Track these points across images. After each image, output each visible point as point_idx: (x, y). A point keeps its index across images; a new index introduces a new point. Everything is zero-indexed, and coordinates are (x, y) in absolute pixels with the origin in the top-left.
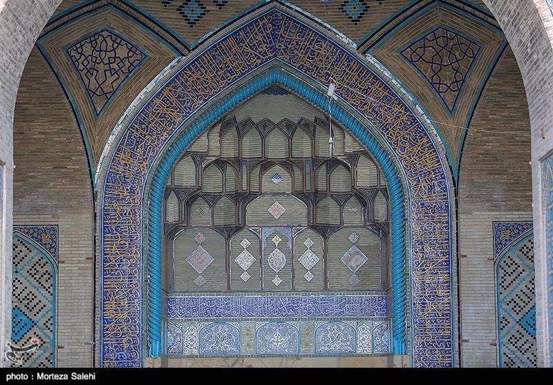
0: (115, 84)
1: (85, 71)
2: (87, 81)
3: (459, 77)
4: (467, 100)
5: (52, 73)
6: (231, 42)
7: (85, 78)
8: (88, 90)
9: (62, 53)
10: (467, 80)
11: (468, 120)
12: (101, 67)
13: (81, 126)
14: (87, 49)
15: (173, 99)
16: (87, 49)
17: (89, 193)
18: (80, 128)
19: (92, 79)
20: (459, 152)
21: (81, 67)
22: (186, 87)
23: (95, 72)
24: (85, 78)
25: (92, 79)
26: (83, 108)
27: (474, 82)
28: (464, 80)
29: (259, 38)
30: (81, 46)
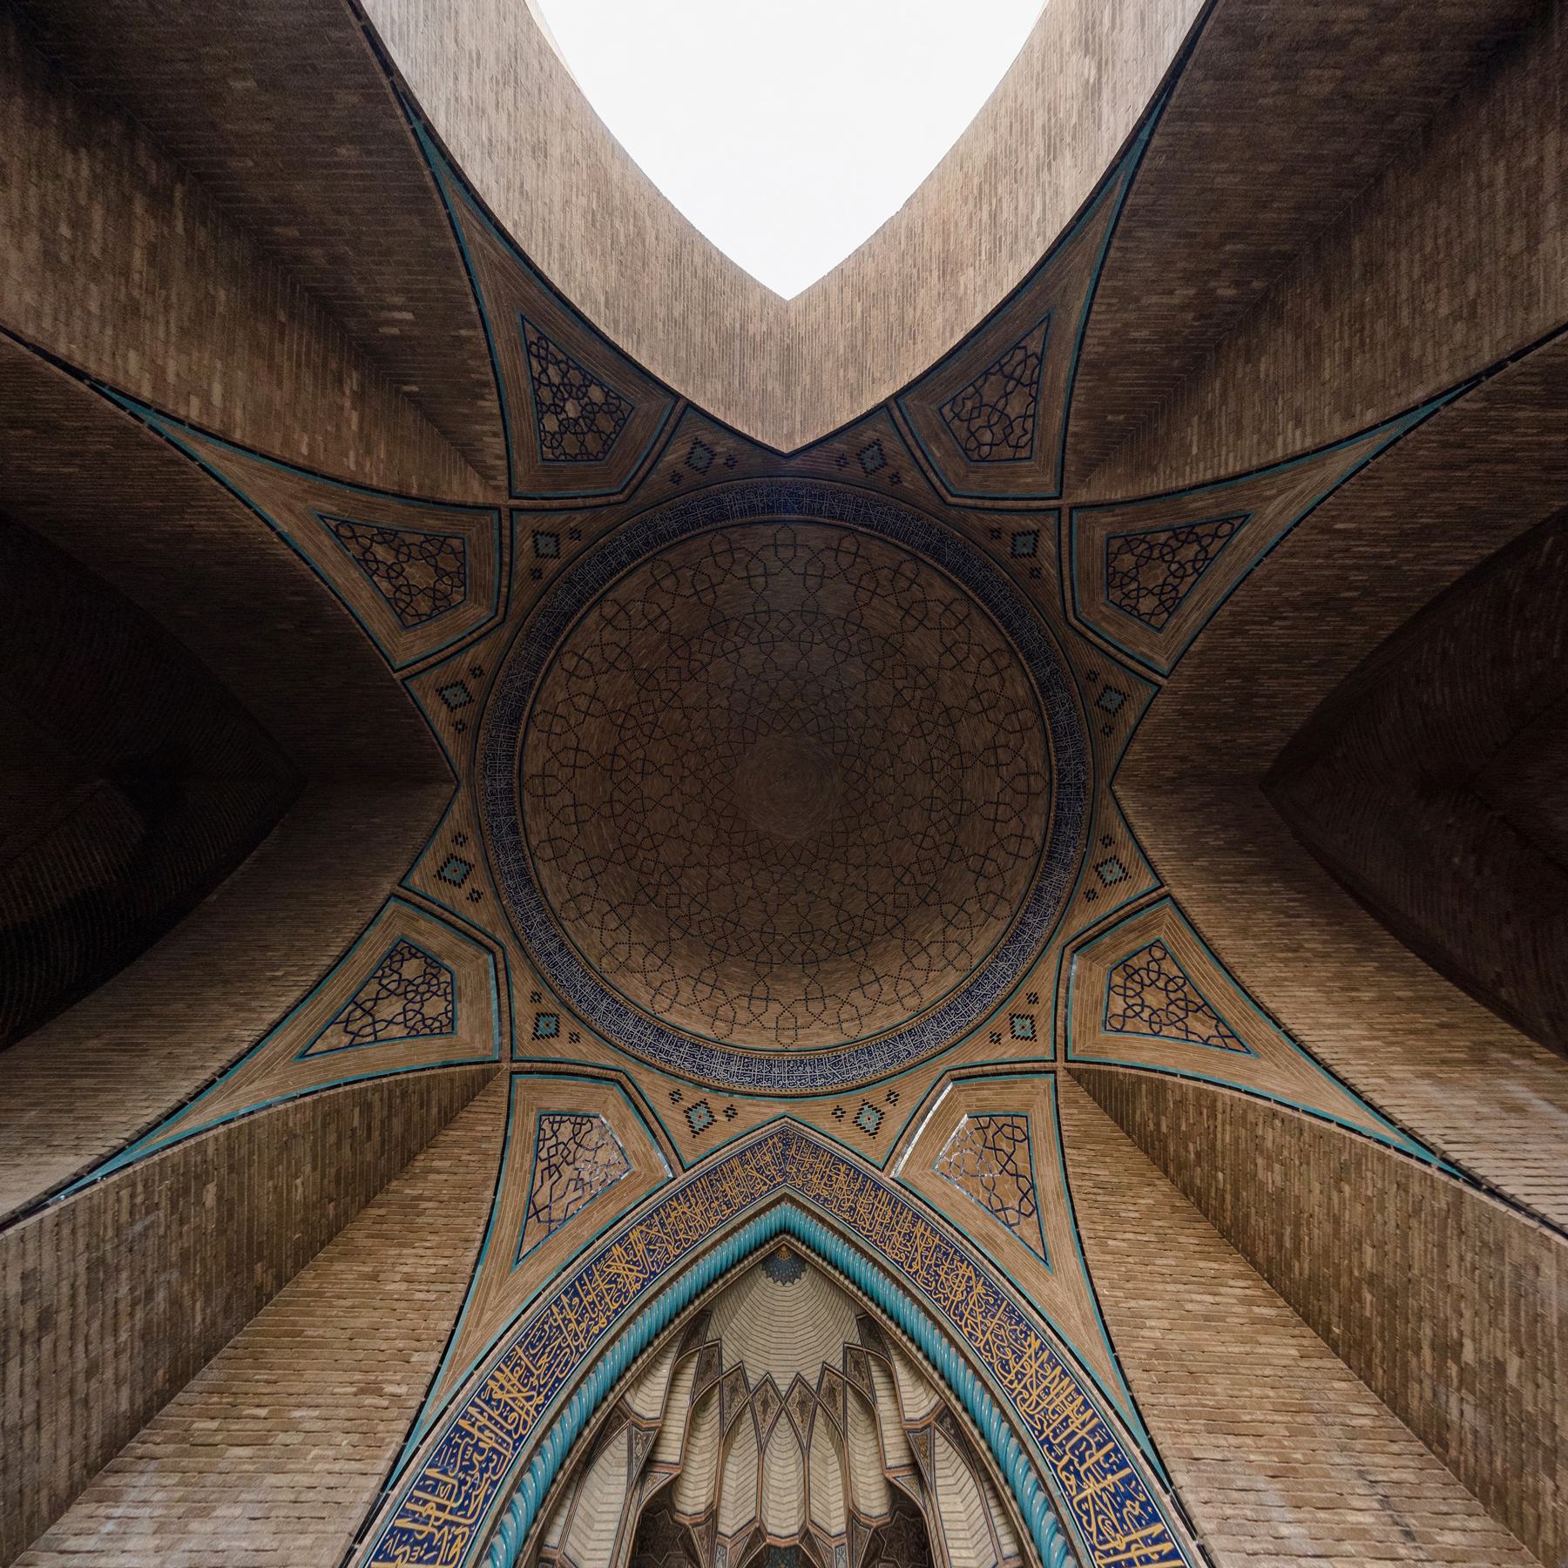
0: (572, 1208)
1: (545, 1164)
2: (538, 1183)
3: (1025, 1186)
4: (1056, 1218)
5: (501, 1132)
6: (736, 1162)
7: (538, 1175)
8: (531, 1200)
9: (533, 1117)
10: (1036, 1181)
11: (1080, 1261)
12: (568, 1172)
13: (480, 1268)
14: (566, 1131)
15: (641, 1246)
16: (566, 1131)
17: (351, 462)
18: (474, 1270)
19: (548, 1184)
20: (1109, 1355)
21: (544, 1154)
22: (663, 1225)
23: (556, 1176)
24: (538, 1175)
25: (548, 1184)
26: (505, 1232)
27: (1049, 1177)
28: (1033, 1186)
29: (768, 1158)
30: (561, 1122)
